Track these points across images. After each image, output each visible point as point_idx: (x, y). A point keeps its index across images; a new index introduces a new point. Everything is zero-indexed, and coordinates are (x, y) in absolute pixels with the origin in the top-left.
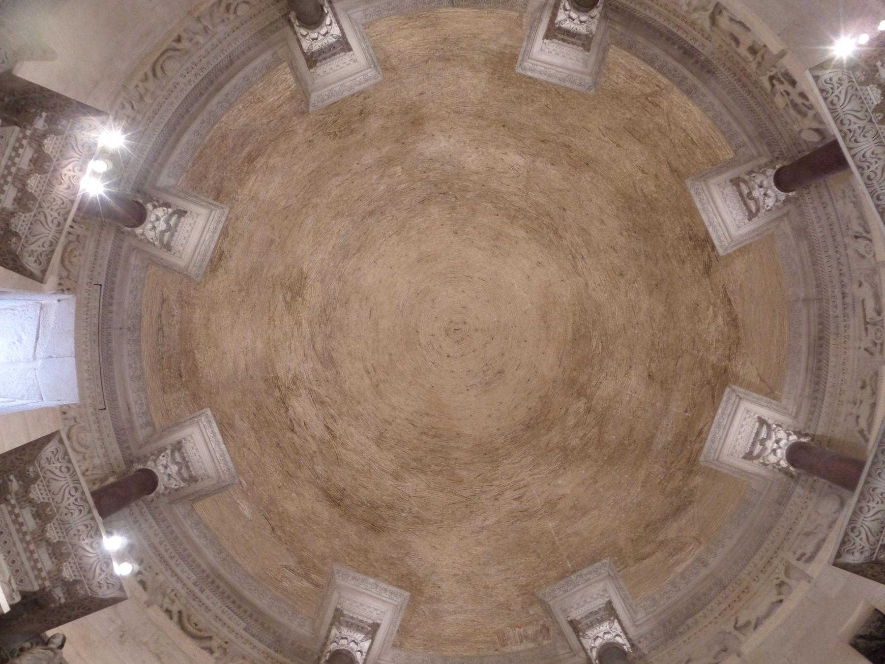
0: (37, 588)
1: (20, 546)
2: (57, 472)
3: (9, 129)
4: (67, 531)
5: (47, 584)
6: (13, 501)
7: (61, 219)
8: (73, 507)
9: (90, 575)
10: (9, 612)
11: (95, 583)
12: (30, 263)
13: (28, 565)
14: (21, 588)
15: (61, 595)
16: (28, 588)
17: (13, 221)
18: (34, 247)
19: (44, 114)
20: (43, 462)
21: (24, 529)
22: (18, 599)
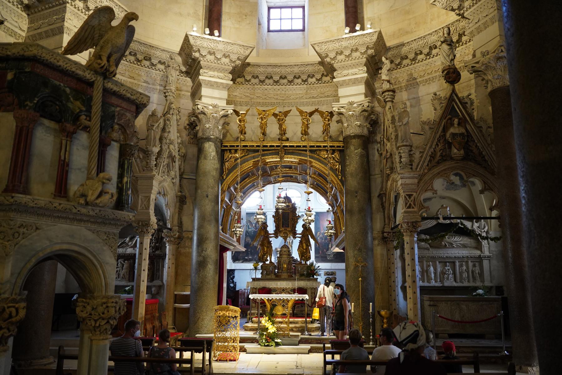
0: (365, 59)
1: (349, 62)
2: (326, 47)
3: (202, 65)
4: (347, 47)
5: (365, 56)
6: (333, 62)
7: (230, 44)
8: (340, 44)
9: (367, 42)
10: (368, 74)
11: (370, 41)
12: (247, 52)
13: (357, 61)
14: (363, 65)
15: (371, 51)
16: (364, 62)
17: (234, 60)
18: (242, 52)
19: (193, 54)
20: (321, 51)
21: (344, 60)
22: (365, 69)
